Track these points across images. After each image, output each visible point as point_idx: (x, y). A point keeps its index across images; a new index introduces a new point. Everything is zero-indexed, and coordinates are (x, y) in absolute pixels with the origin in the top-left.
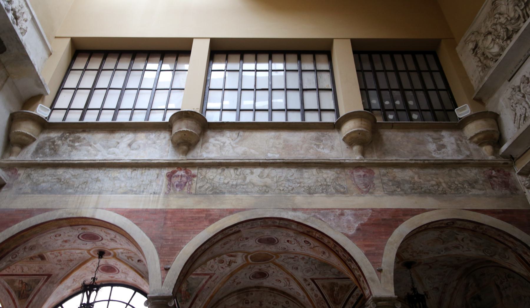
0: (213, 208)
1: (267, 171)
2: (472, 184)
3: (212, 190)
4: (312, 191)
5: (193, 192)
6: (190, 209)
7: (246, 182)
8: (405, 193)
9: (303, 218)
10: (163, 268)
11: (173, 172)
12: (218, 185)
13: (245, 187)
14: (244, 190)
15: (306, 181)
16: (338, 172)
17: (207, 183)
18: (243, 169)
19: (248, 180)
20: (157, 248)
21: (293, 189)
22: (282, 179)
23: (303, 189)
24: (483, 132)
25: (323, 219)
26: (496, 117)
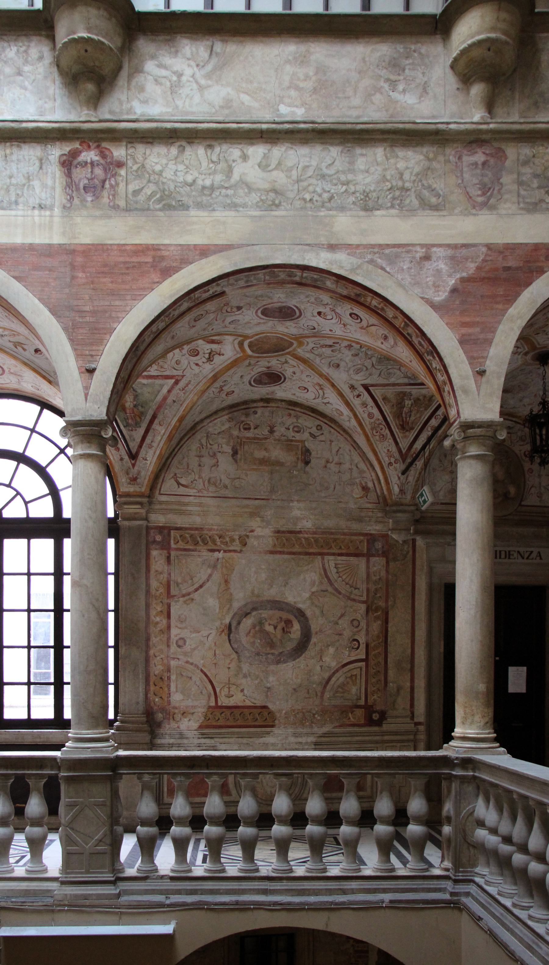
0: (167, 242)
1: (278, 152)
3: (160, 200)
4: (370, 204)
5: (122, 203)
6: (118, 245)
7: (233, 181)
9: (349, 267)
10: (84, 370)
11: (74, 154)
12: (172, 187)
13: (230, 192)
14: (229, 201)
15: (360, 177)
16: (431, 155)
17: (149, 181)
18: (225, 147)
19: (236, 176)
20: (65, 329)
21: (331, 199)
22: (310, 173)
23: (352, 199)
25: (388, 269)
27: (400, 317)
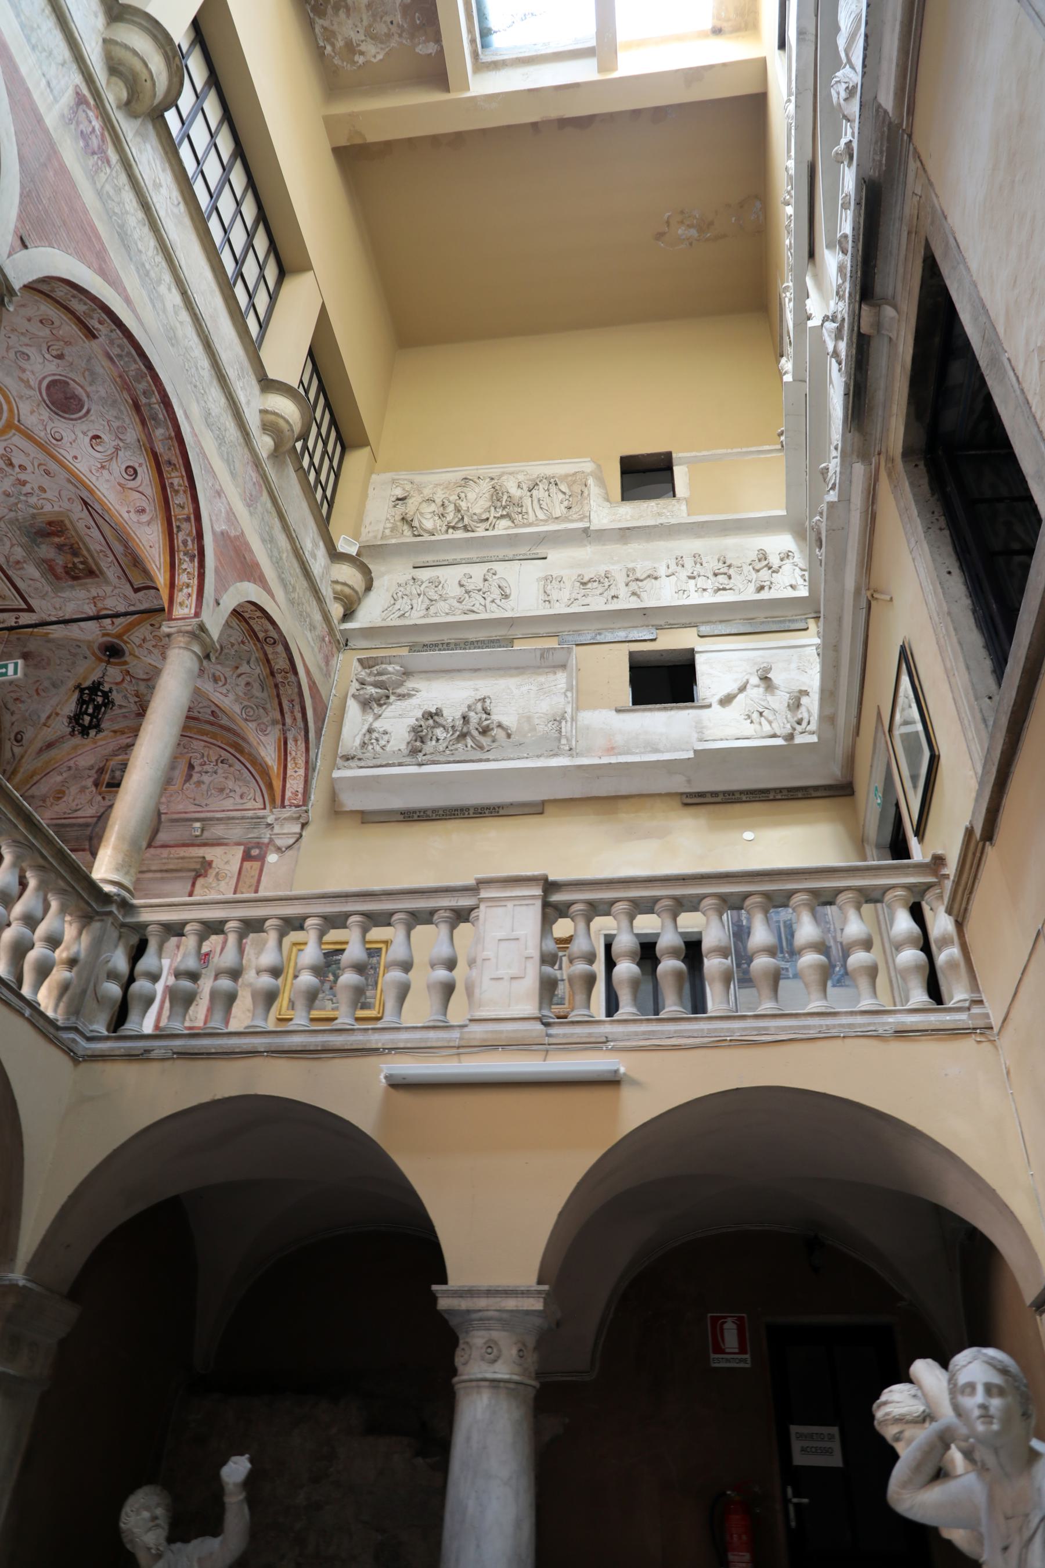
2: (312, 628)
8: (271, 557)
24: (353, 589)
26: (369, 588)
27: (189, 509)
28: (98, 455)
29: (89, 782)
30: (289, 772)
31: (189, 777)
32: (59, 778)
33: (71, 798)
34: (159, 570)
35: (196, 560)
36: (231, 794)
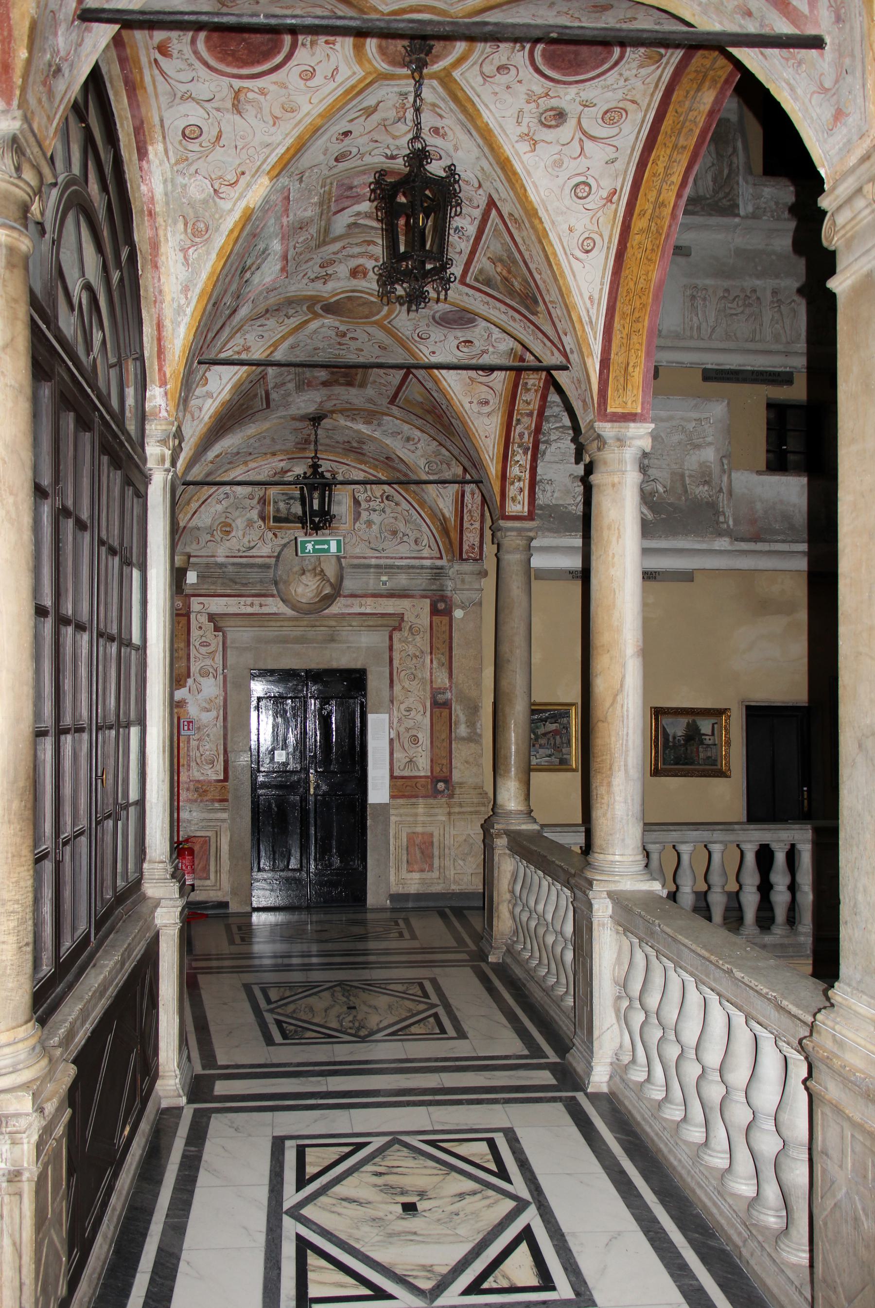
28: (460, 354)
29: (254, 514)
30: (466, 525)
31: (357, 516)
32: (219, 508)
33: (240, 533)
34: (492, 460)
35: (529, 453)
36: (405, 538)
